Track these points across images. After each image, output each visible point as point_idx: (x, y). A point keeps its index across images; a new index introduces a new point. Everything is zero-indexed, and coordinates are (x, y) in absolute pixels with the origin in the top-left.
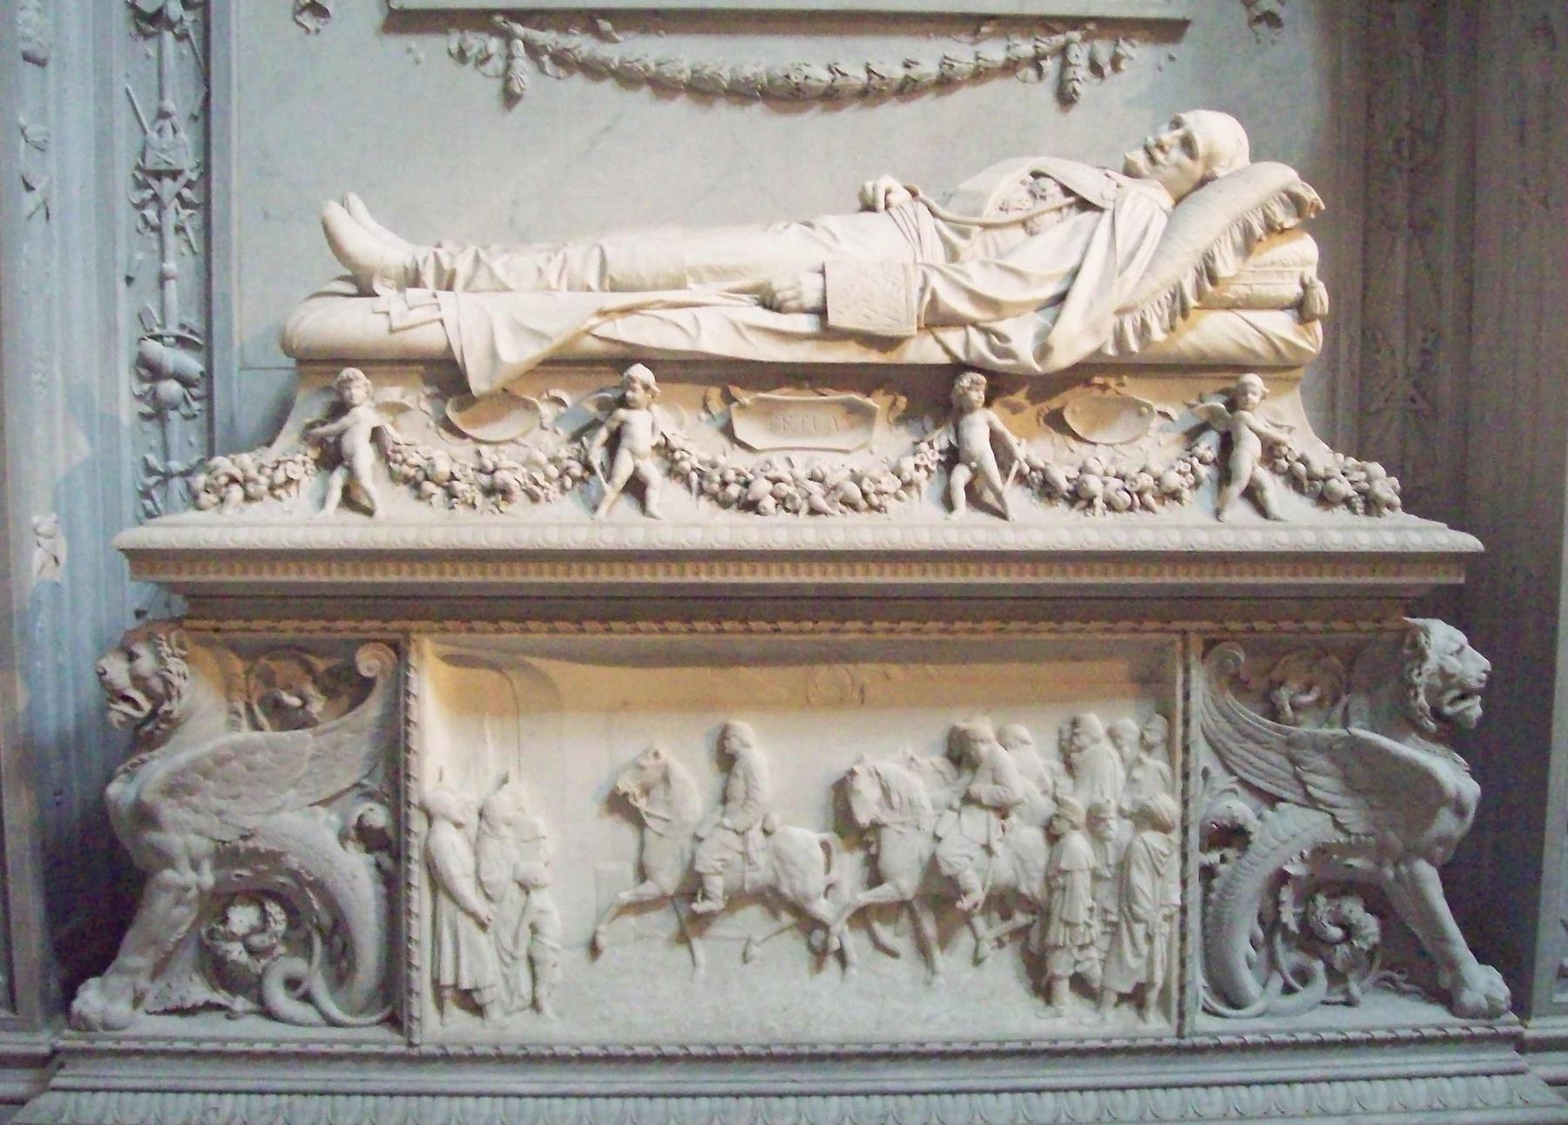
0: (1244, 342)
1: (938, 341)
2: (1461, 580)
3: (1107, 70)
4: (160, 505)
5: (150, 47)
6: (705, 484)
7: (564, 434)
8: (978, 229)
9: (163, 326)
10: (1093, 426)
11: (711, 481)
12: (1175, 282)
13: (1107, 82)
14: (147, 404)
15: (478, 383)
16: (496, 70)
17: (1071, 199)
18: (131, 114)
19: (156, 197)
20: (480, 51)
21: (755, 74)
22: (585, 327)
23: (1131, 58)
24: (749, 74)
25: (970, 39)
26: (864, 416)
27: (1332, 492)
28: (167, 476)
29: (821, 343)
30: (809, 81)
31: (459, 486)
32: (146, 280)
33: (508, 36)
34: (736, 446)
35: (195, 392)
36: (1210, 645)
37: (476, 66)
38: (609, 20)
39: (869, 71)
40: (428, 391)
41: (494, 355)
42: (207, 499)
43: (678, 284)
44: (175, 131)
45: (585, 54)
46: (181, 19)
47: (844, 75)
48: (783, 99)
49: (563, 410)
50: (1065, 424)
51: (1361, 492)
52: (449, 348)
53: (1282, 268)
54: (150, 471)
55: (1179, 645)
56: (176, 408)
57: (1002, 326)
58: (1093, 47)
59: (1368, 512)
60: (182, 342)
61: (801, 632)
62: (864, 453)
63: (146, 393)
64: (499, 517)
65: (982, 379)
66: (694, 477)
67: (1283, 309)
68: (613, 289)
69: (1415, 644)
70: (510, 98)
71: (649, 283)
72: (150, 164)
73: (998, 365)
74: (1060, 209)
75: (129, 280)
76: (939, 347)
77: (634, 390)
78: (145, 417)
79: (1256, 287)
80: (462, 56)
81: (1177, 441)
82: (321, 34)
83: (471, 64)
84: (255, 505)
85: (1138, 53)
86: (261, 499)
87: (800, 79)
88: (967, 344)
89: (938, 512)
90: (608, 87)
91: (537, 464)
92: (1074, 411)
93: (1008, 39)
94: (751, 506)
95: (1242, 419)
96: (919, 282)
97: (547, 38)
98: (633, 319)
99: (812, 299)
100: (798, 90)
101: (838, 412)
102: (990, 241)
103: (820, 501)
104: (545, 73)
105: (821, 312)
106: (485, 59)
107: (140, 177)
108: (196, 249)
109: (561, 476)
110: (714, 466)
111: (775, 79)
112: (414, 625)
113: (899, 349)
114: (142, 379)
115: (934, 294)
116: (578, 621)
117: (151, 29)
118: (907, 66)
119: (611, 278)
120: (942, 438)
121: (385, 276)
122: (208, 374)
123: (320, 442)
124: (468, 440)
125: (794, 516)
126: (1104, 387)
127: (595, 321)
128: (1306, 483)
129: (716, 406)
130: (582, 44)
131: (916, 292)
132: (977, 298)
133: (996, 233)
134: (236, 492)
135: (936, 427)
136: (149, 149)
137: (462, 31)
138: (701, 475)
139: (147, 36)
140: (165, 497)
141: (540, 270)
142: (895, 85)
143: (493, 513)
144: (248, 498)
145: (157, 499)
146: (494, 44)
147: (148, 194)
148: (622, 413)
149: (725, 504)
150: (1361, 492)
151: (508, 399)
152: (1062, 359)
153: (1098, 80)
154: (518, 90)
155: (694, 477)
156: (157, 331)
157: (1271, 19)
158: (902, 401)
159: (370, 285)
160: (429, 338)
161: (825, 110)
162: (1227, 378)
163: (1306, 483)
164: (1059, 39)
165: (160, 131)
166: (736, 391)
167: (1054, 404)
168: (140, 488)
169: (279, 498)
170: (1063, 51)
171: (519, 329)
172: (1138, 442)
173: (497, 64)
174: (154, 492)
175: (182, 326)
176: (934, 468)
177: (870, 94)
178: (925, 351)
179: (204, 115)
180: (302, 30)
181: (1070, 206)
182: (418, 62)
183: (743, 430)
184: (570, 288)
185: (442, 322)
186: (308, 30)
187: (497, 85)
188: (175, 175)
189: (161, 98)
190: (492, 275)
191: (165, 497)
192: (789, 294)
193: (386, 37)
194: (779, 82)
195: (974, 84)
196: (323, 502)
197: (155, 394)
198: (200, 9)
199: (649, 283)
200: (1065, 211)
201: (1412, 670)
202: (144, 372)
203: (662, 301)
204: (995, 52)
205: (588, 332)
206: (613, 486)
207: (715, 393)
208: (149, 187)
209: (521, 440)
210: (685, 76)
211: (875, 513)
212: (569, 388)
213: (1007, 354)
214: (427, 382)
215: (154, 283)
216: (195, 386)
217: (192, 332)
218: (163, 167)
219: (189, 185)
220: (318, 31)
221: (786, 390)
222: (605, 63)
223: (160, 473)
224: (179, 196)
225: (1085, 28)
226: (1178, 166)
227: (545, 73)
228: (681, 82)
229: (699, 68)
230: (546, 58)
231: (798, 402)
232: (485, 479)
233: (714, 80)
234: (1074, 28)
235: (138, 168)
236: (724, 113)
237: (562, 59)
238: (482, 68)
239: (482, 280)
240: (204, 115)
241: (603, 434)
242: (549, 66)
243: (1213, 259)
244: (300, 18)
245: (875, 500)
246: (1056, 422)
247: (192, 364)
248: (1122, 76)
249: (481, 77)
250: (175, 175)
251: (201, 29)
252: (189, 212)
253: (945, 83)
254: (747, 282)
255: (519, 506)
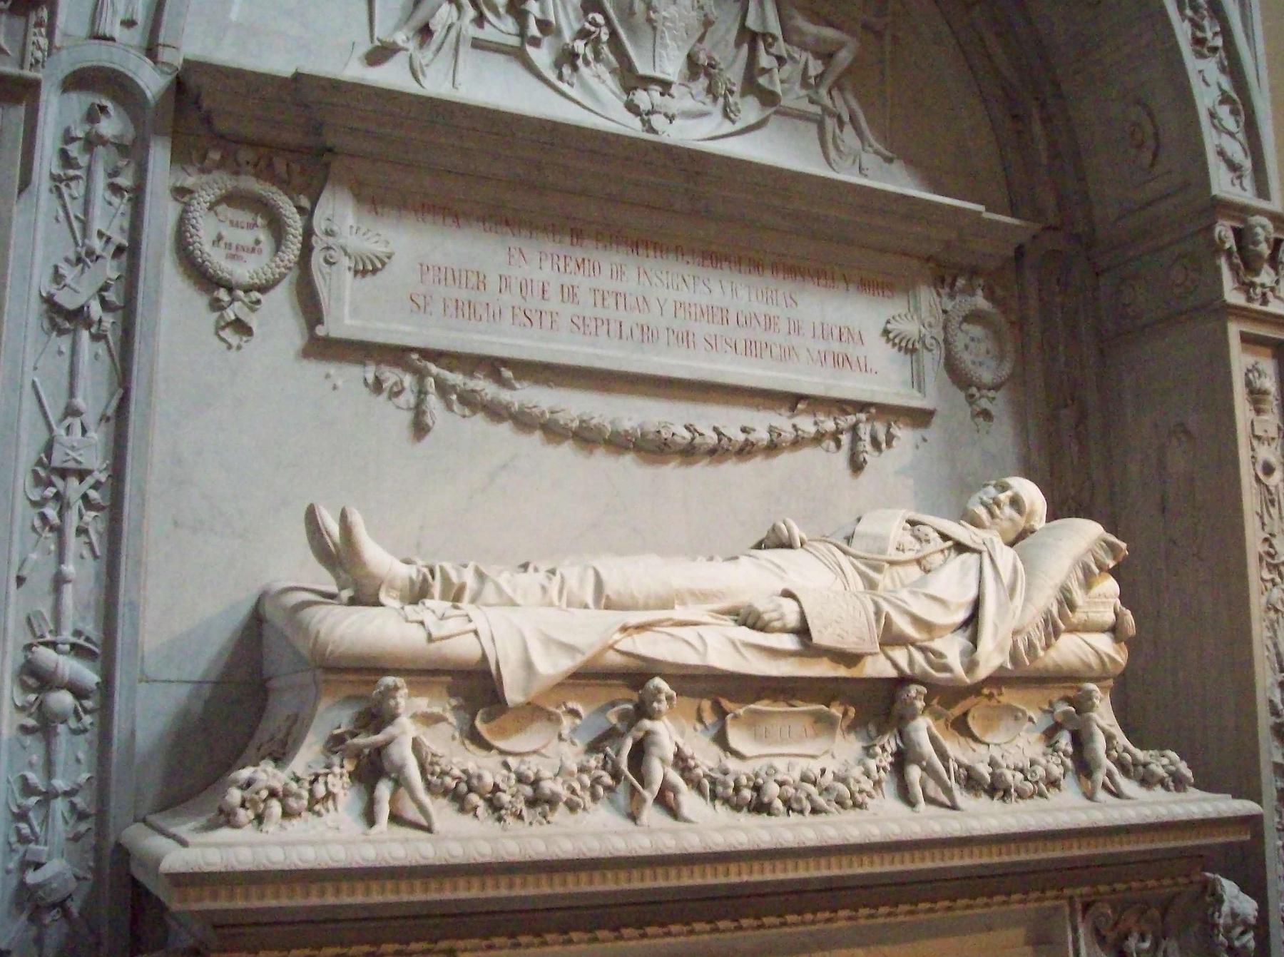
0: (1086, 659)
1: (889, 658)
2: (1248, 837)
3: (884, 445)
4: (37, 829)
5: (64, 343)
6: (720, 789)
7: (581, 746)
8: (887, 566)
9: (57, 631)
10: (986, 729)
11: (725, 785)
12: (1045, 609)
13: (883, 455)
14: (30, 715)
15: (513, 694)
16: (408, 401)
17: (950, 543)
18: (36, 408)
19: (58, 496)
20: (396, 384)
21: (632, 428)
22: (610, 642)
23: (899, 438)
24: (628, 428)
25: (789, 414)
26: (825, 723)
27: (1153, 774)
28: (48, 796)
29: (805, 659)
30: (675, 437)
31: (505, 798)
32: (40, 580)
33: (421, 374)
34: (729, 754)
35: (89, 704)
36: (1087, 907)
37: (390, 398)
38: (510, 369)
39: (719, 434)
40: (454, 702)
41: (528, 666)
42: (244, 815)
43: (666, 604)
44: (84, 431)
45: (489, 397)
46: (100, 321)
47: (701, 434)
48: (653, 452)
49: (578, 721)
50: (968, 728)
51: (1171, 774)
52: (484, 658)
53: (1104, 600)
54: (28, 789)
55: (1067, 910)
56: (64, 721)
57: (937, 644)
58: (873, 427)
59: (1177, 790)
60: (77, 650)
61: (803, 923)
62: (828, 757)
63: (32, 705)
64: (546, 828)
65: (924, 690)
66: (706, 782)
67: (1103, 631)
68: (607, 607)
69: (1214, 893)
70: (420, 428)
71: (641, 602)
72: (57, 461)
73: (938, 679)
74: (942, 551)
75: (20, 580)
76: (889, 664)
77: (659, 701)
78: (25, 729)
79: (1091, 615)
80: (377, 386)
81: (1040, 739)
82: (242, 350)
83: (385, 395)
84: (295, 822)
85: (904, 435)
86: (300, 814)
87: (669, 436)
88: (911, 662)
89: (900, 808)
90: (505, 428)
91: (571, 774)
92: (974, 717)
93: (815, 415)
94: (760, 807)
95: (1089, 719)
96: (871, 609)
97: (456, 378)
98: (647, 636)
99: (792, 620)
100: (665, 444)
101: (807, 722)
102: (895, 575)
103: (821, 801)
104: (452, 411)
105: (803, 631)
106: (396, 393)
107: (42, 473)
108: (98, 553)
109: (592, 786)
110: (726, 773)
111: (648, 434)
112: (461, 944)
113: (860, 666)
114: (26, 688)
115: (888, 618)
116: (616, 929)
117: (67, 325)
118: (744, 430)
119: (608, 597)
120: (891, 743)
121: (392, 587)
122: (107, 685)
123: (357, 754)
124: (494, 752)
125: (800, 816)
126: (990, 696)
127: (617, 636)
128: (1132, 768)
129: (709, 718)
130: (485, 387)
131: (872, 616)
132: (917, 621)
133: (899, 569)
134: (276, 807)
135: (881, 732)
136: (56, 446)
137: (378, 363)
138: (713, 782)
139: (61, 332)
140: (45, 821)
141: (544, 589)
142: (737, 447)
143: (541, 824)
144: (287, 814)
145: (35, 823)
146: (408, 380)
147: (50, 492)
148: (647, 724)
149: (737, 808)
150: (1171, 774)
151: (535, 712)
152: (983, 672)
153: (876, 454)
154: (430, 423)
155: (706, 782)
156: (49, 637)
157: (986, 415)
158: (852, 712)
159: (377, 595)
160: (464, 648)
161: (681, 464)
162: (1066, 688)
163: (1132, 768)
164: (851, 419)
165: (68, 428)
166: (726, 704)
167: (956, 711)
168: (15, 810)
169: (319, 814)
170: (854, 429)
171: (549, 642)
172: (1015, 742)
173: (408, 398)
174: (31, 814)
175: (78, 633)
176: (889, 768)
177: (719, 452)
178: (878, 667)
179: (119, 418)
180: (224, 346)
181: (949, 548)
182: (335, 388)
183: (736, 738)
184: (569, 604)
185: (476, 632)
186: (230, 347)
187: (408, 417)
188: (82, 474)
189: (72, 394)
190: (499, 589)
191: (45, 821)
192: (775, 615)
193: (305, 363)
194: (651, 436)
195: (792, 451)
196: (370, 817)
197: (41, 705)
198: (120, 312)
199: (641, 602)
200: (946, 552)
201: (1213, 913)
202: (31, 681)
203: (668, 620)
204: (807, 425)
205: (611, 647)
206: (652, 792)
207: (706, 704)
208: (51, 484)
209: (543, 751)
210: (575, 424)
211: (858, 810)
212: (579, 699)
213: (946, 668)
214: (452, 694)
215: (47, 586)
216: (87, 697)
217: (88, 639)
218: (71, 465)
219: (97, 486)
220: (239, 347)
221: (766, 702)
222: (507, 407)
223: (39, 793)
224: (85, 497)
225: (868, 412)
226: (1011, 520)
227: (452, 411)
228: (570, 429)
229: (585, 418)
230: (454, 397)
231: (780, 712)
232: (528, 790)
233: (599, 429)
234: (861, 411)
235: (40, 463)
236: (602, 461)
237: (470, 401)
238: (395, 400)
239: (489, 593)
240: (119, 418)
241: (628, 744)
242: (456, 407)
243: (1069, 591)
244: (223, 334)
245: (859, 798)
246: (961, 727)
247: (89, 675)
248: (892, 451)
249: (394, 408)
250: (82, 474)
251: (119, 332)
252: (93, 514)
253: (773, 448)
254: (726, 604)
255: (561, 812)
